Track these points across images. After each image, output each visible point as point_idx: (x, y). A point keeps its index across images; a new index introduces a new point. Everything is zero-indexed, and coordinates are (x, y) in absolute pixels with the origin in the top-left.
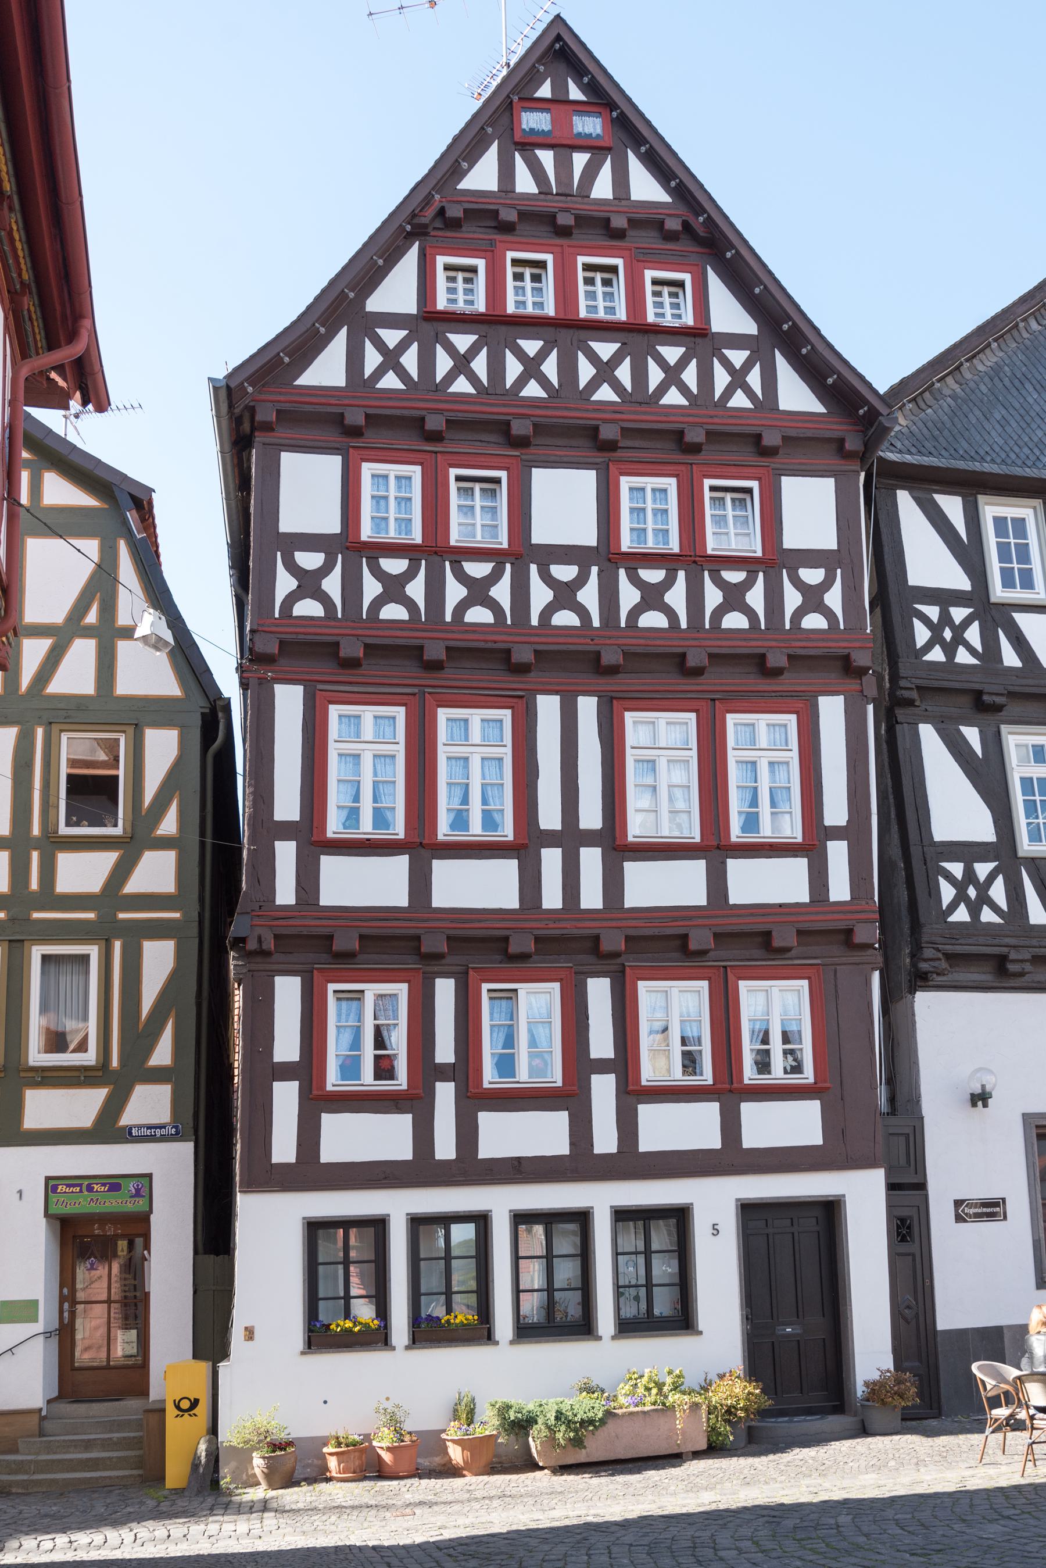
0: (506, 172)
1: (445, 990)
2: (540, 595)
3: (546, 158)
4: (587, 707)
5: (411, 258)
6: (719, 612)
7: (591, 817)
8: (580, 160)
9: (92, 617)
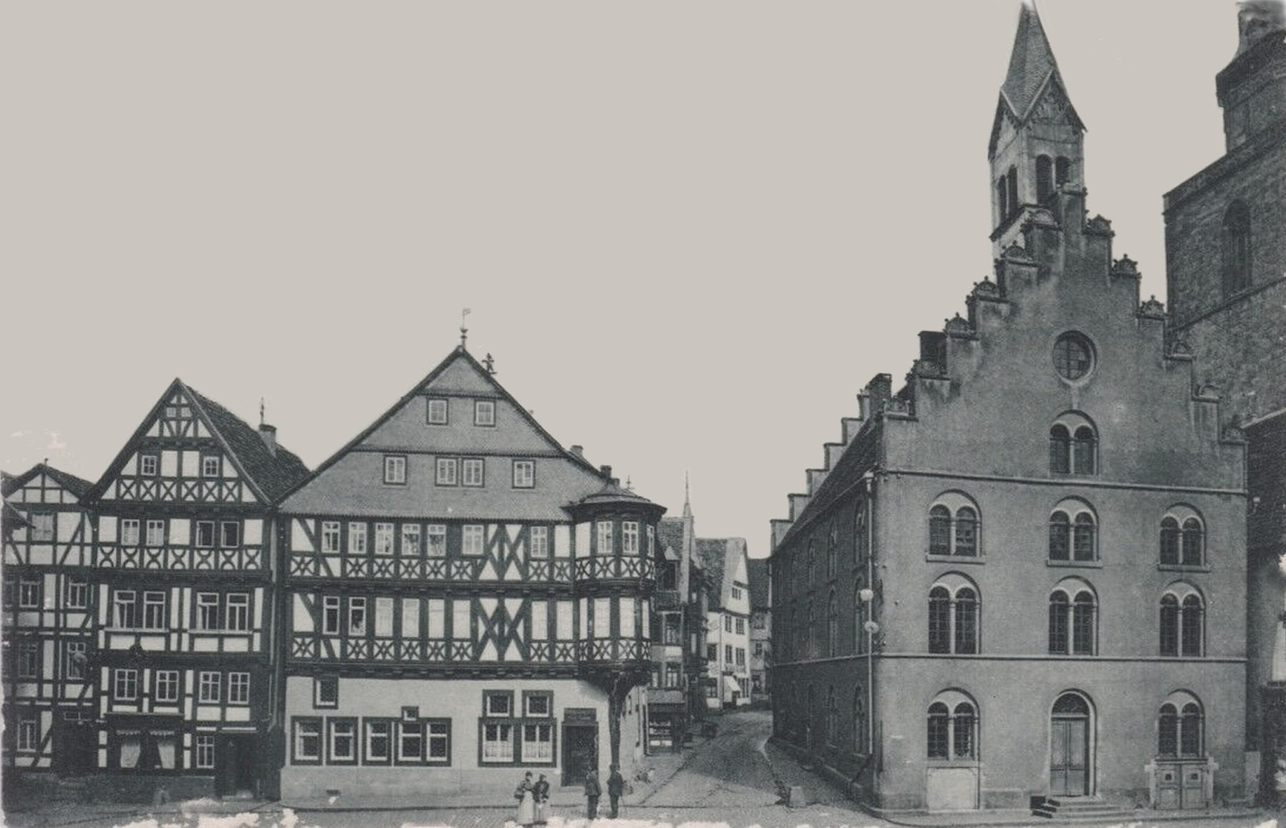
0: (161, 431)
1: (147, 672)
2: (171, 559)
3: (173, 424)
4: (187, 592)
5: (135, 456)
6: (224, 564)
8: (184, 424)
9: (78, 540)
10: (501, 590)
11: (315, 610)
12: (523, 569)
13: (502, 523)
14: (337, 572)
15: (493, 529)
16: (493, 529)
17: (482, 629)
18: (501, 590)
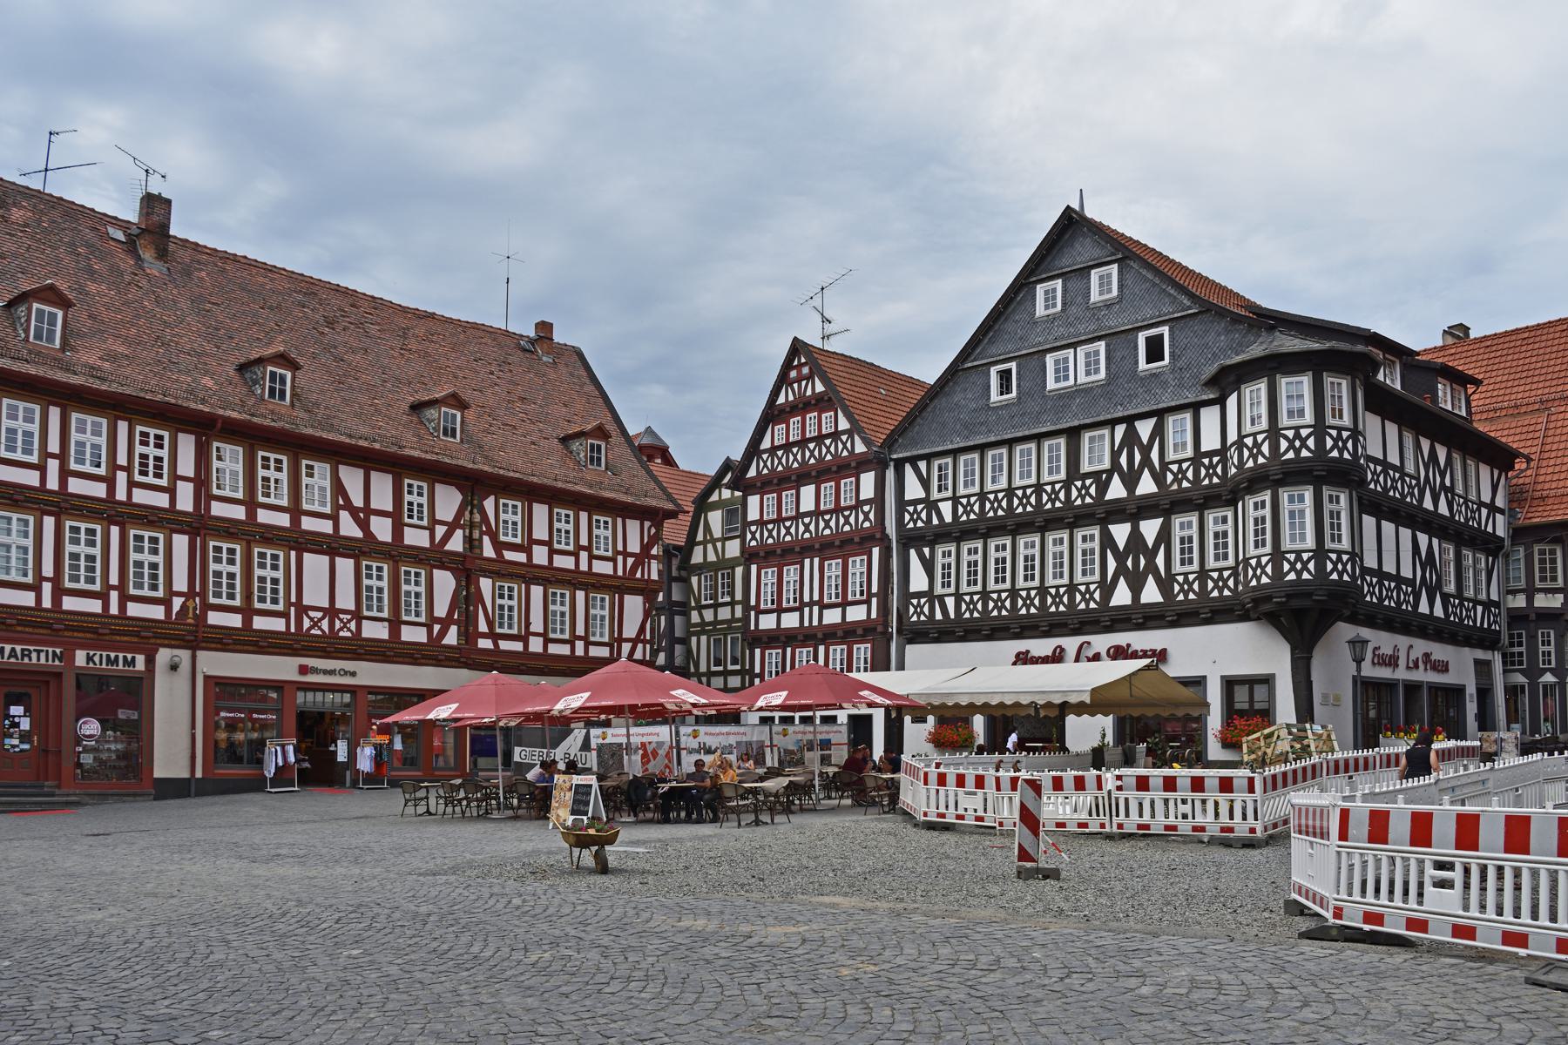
4: (816, 560)
7: (816, 597)
10: (1134, 510)
11: (929, 566)
12: (1158, 478)
13: (1130, 420)
14: (948, 518)
15: (1120, 430)
16: (1120, 430)
17: (1112, 565)
18: (1134, 510)
